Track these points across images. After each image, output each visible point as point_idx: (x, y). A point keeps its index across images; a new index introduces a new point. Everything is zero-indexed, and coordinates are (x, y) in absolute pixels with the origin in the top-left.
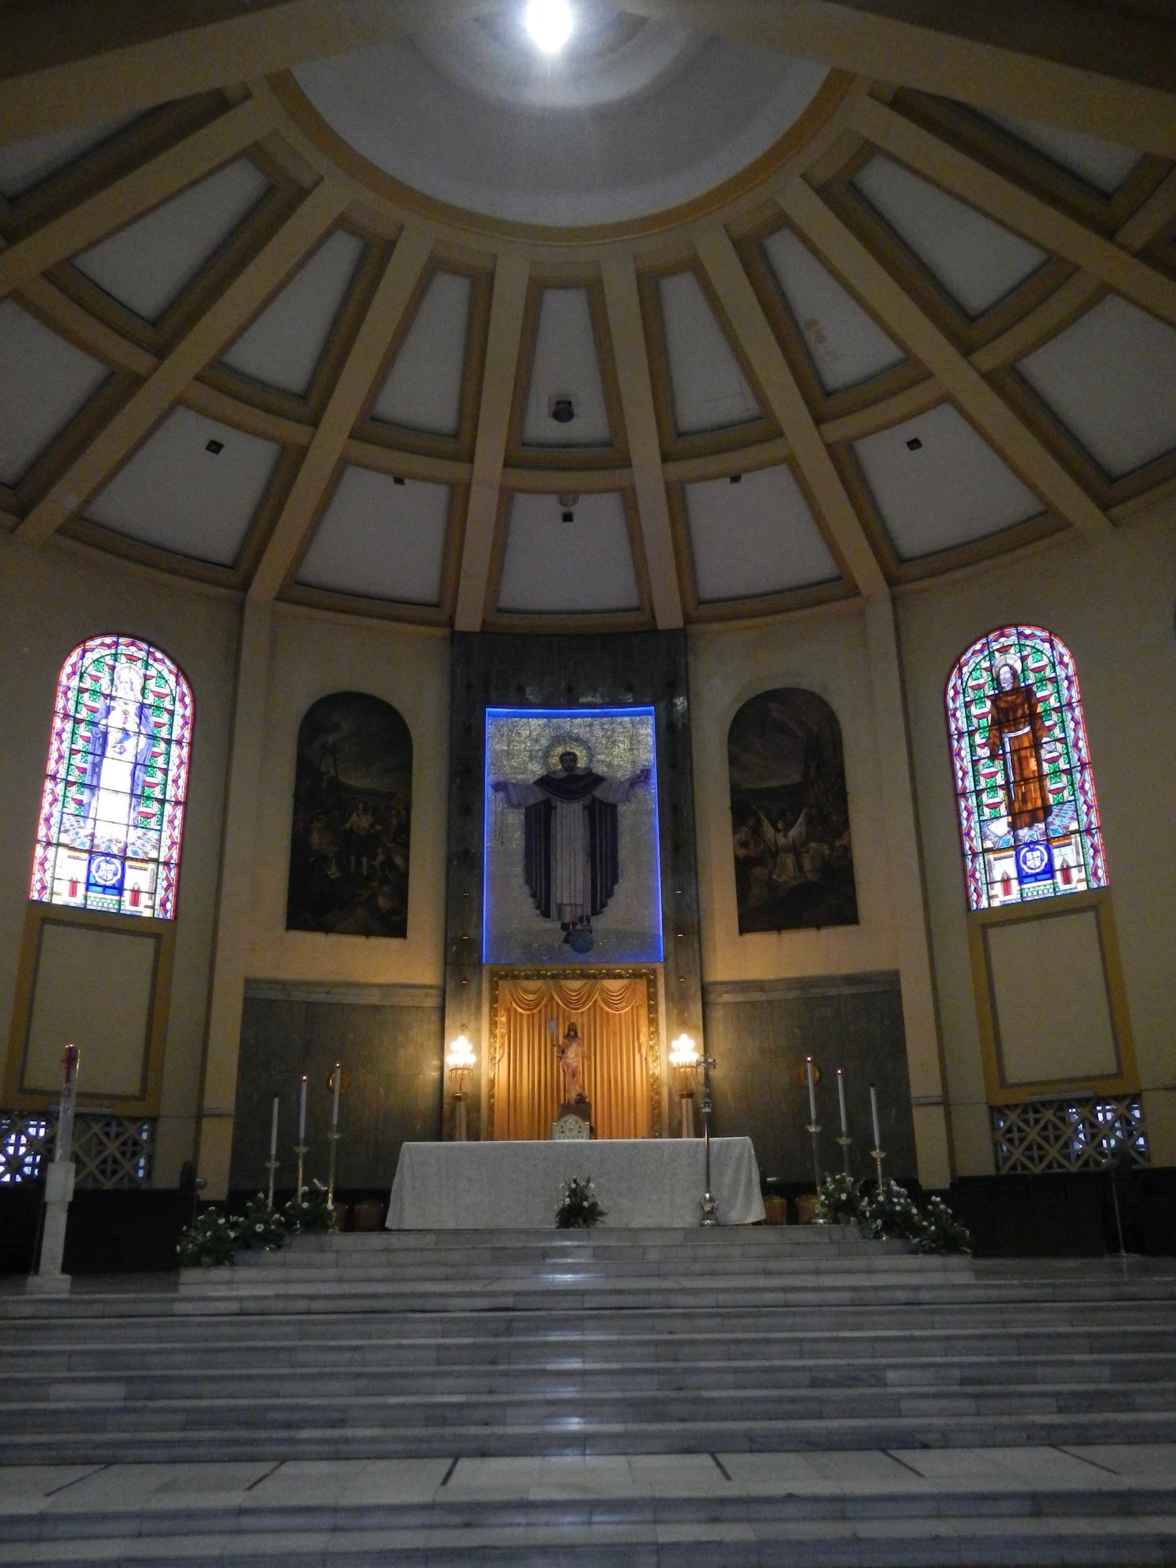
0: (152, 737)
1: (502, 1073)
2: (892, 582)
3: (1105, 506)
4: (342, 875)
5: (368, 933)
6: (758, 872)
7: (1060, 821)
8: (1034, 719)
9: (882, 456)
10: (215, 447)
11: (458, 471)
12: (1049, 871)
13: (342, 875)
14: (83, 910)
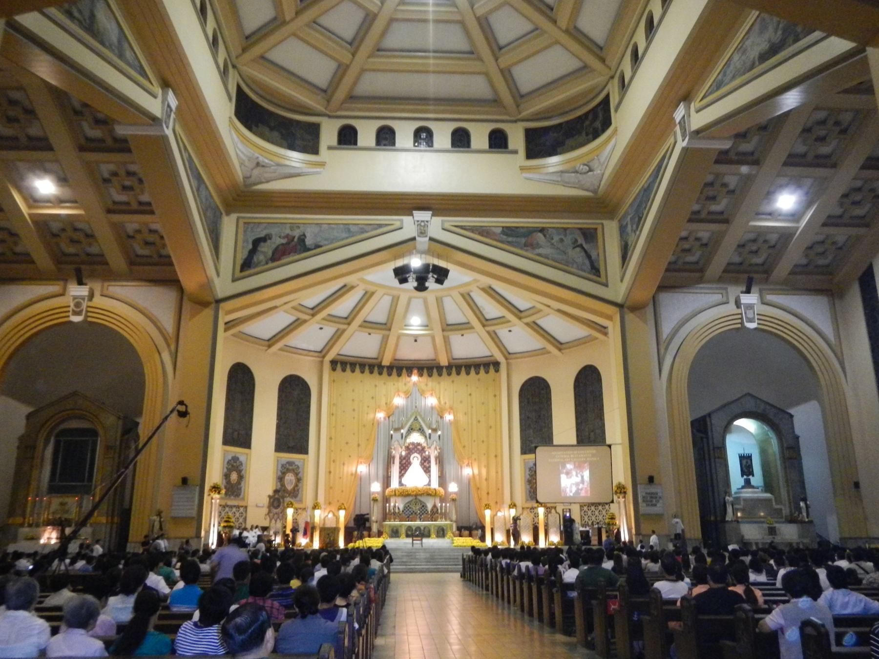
2: (506, 359)
3: (560, 350)
9: (502, 332)
10: (321, 328)
11: (386, 332)
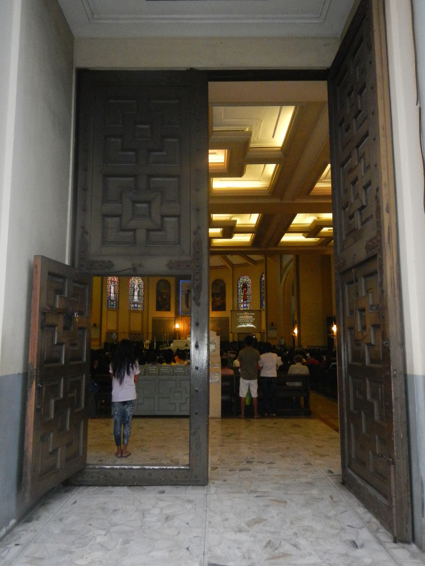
0: (140, 288)
1: (182, 328)
3: (254, 264)
4: (163, 305)
5: (166, 311)
6: (214, 304)
7: (248, 301)
8: (247, 288)
12: (246, 307)
13: (163, 305)
14: (134, 310)
